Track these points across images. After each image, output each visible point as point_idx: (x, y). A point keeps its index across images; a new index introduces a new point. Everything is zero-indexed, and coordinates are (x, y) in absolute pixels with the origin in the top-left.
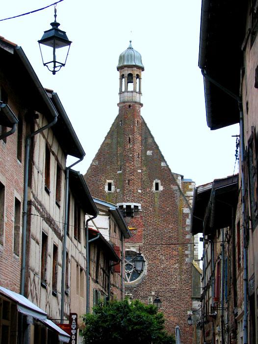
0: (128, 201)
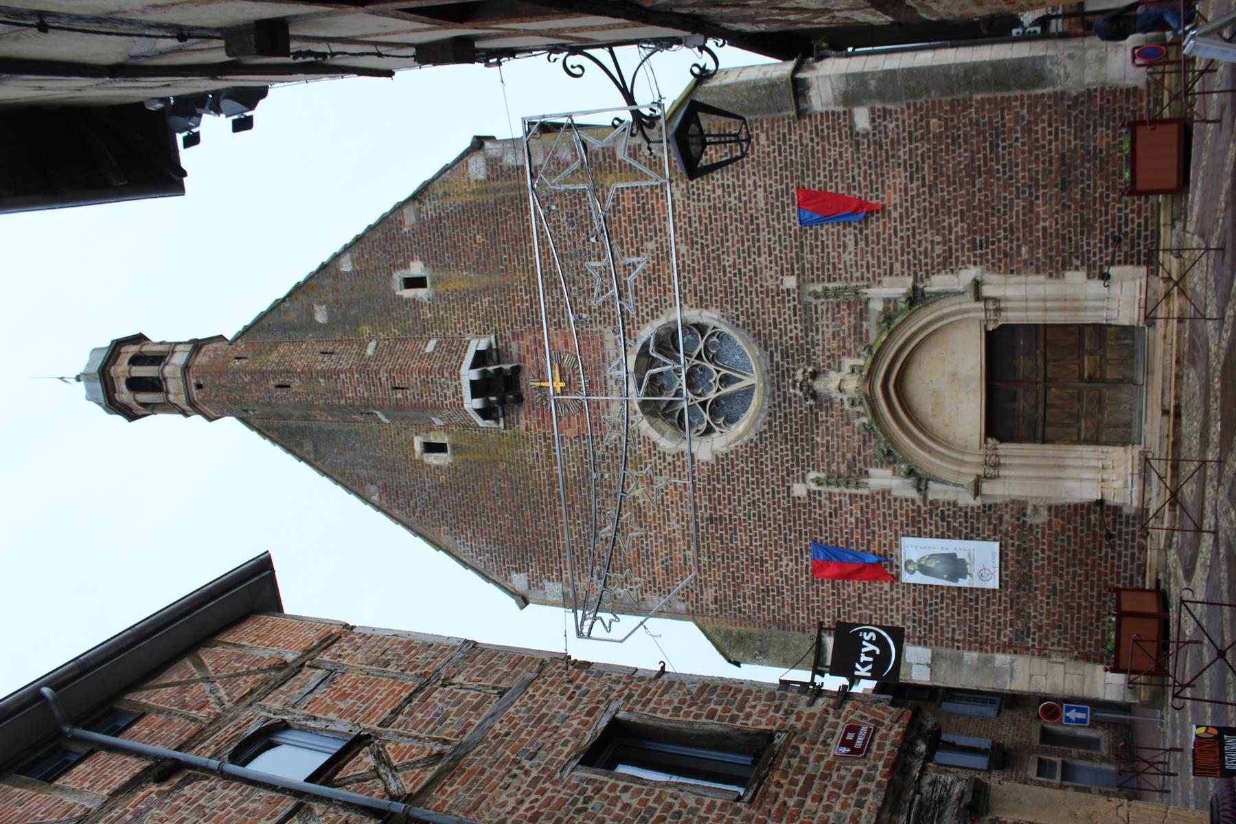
0: (458, 392)
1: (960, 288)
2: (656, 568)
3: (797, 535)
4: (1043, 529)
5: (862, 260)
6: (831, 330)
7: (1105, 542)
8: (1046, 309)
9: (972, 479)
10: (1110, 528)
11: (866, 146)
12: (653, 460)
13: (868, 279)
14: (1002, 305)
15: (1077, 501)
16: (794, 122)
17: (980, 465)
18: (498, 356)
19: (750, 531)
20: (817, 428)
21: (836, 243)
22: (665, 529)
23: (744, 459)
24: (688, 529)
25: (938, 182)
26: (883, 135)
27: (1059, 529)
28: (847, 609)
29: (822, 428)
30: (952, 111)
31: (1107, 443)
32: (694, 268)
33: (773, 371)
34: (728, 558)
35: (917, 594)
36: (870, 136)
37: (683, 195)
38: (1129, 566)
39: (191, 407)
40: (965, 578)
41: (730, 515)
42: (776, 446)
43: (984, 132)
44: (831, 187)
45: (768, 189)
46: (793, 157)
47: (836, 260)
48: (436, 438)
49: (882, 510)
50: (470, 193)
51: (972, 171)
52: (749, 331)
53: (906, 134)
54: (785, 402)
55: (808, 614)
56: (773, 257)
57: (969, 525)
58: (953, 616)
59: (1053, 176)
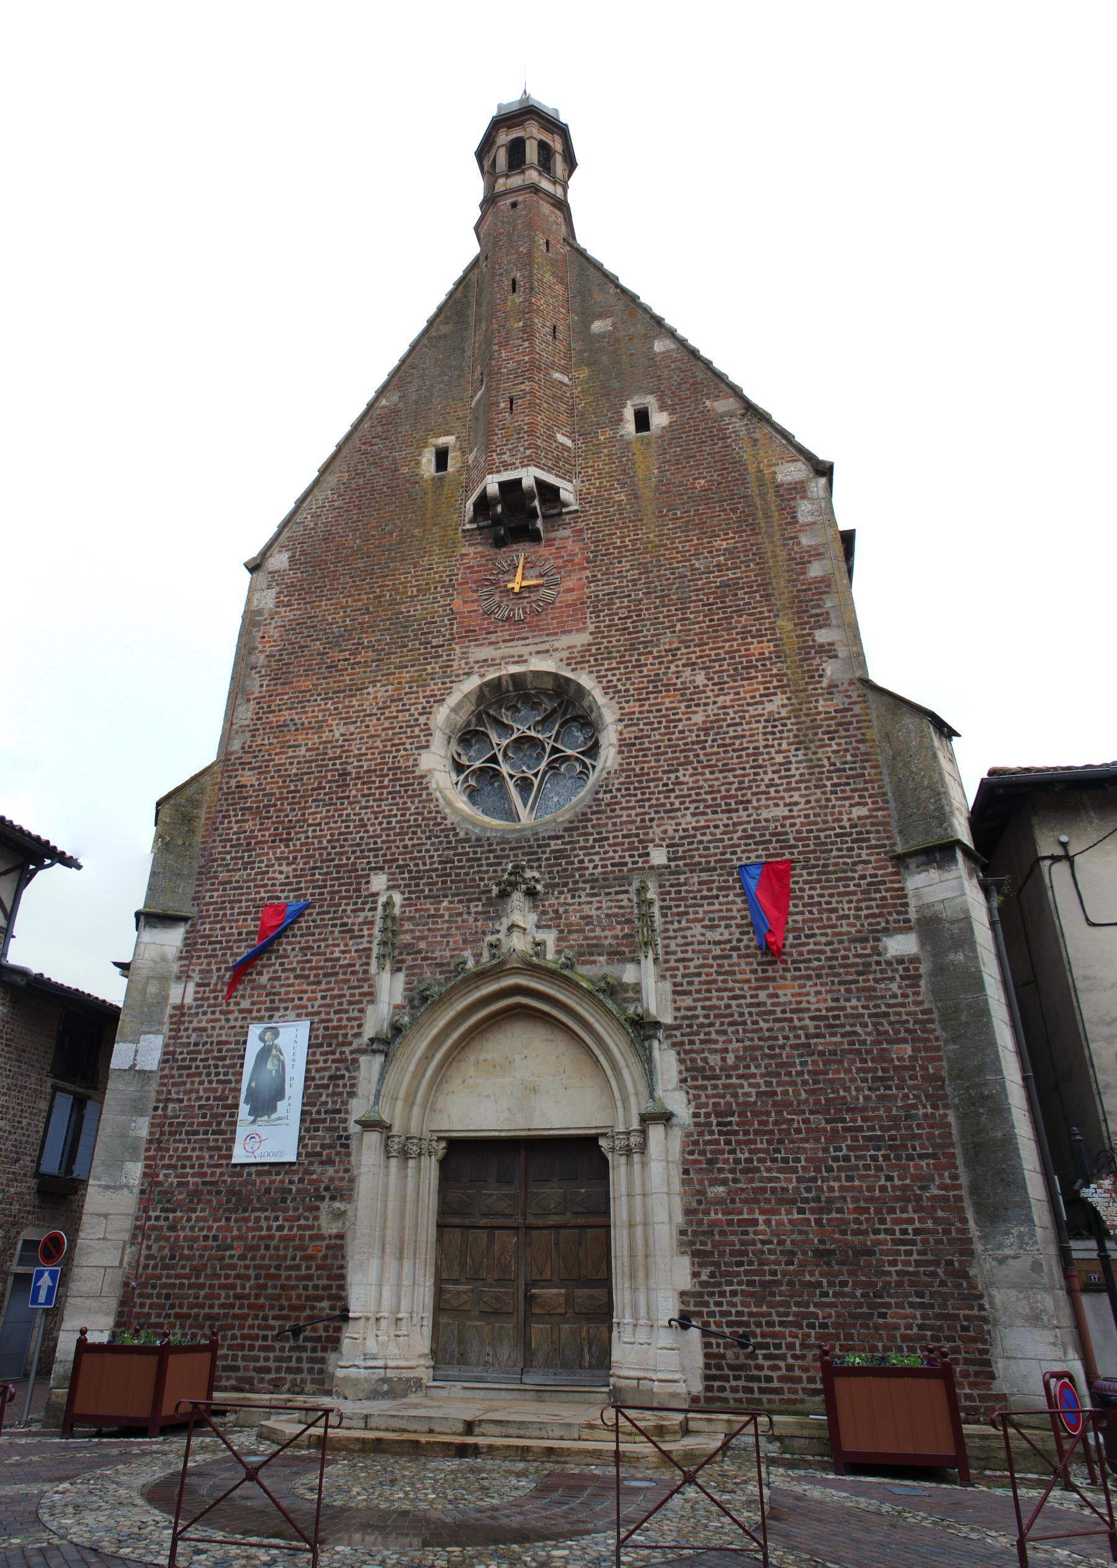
0: (506, 466)
1: (659, 1093)
2: (286, 713)
3: (320, 883)
4: (311, 1228)
5: (693, 951)
6: (594, 913)
7: (288, 1325)
8: (631, 1226)
9: (385, 1117)
10: (308, 1333)
11: (860, 951)
12: (421, 700)
13: (667, 961)
14: (636, 1158)
15: (349, 1279)
16: (886, 853)
17: (407, 1129)
18: (553, 516)
19: (326, 824)
20: (461, 901)
21: (716, 915)
22: (334, 719)
23: (420, 810)
24: (332, 747)
25: (816, 1057)
26: (879, 976)
27: (310, 1252)
28: (220, 953)
29: (461, 908)
30: (927, 1078)
31: (436, 1325)
32: (673, 733)
33: (537, 840)
34: (294, 798)
35: (233, 1046)
36: (876, 958)
37: (771, 713)
38: (252, 1364)
39: (489, 202)
40: (250, 1114)
41: (348, 797)
42: (436, 850)
43: (897, 1127)
44: (796, 906)
45: (788, 822)
46: (835, 853)
47: (691, 916)
48: (454, 458)
49: (347, 992)
50: (758, 467)
51: (836, 1109)
52: (590, 807)
53: (884, 1009)
54: (496, 857)
55: (216, 903)
56: (692, 832)
57: (323, 1116)
58: (199, 1098)
59: (837, 1236)
